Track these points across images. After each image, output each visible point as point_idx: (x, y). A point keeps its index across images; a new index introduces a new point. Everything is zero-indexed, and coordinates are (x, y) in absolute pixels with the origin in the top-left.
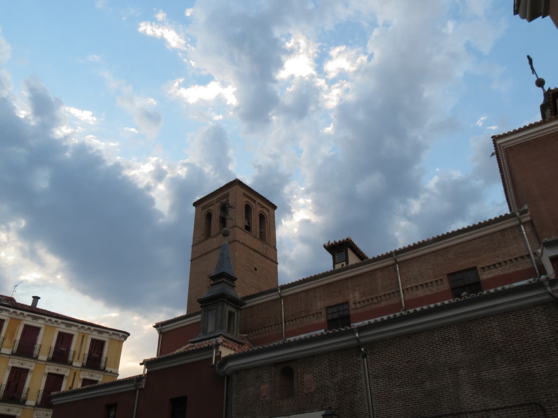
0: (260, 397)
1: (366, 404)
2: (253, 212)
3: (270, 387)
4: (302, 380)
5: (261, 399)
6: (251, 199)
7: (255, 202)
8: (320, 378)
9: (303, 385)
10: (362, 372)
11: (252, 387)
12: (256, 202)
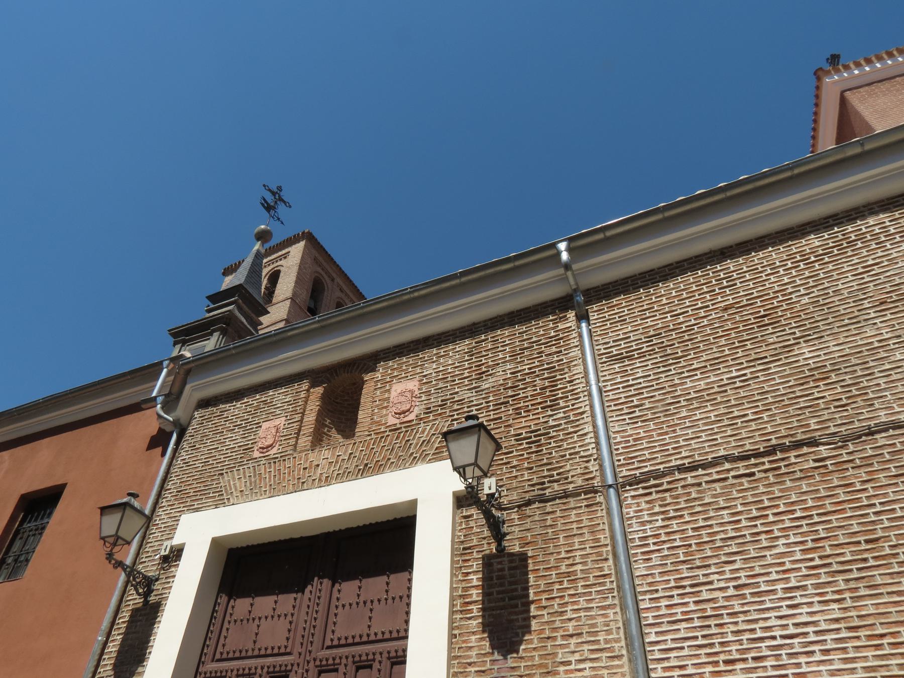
1: (589, 428)
2: (326, 293)
3: (288, 424)
4: (386, 396)
6: (327, 273)
7: (333, 280)
8: (441, 385)
9: (386, 407)
10: (576, 352)
12: (336, 281)
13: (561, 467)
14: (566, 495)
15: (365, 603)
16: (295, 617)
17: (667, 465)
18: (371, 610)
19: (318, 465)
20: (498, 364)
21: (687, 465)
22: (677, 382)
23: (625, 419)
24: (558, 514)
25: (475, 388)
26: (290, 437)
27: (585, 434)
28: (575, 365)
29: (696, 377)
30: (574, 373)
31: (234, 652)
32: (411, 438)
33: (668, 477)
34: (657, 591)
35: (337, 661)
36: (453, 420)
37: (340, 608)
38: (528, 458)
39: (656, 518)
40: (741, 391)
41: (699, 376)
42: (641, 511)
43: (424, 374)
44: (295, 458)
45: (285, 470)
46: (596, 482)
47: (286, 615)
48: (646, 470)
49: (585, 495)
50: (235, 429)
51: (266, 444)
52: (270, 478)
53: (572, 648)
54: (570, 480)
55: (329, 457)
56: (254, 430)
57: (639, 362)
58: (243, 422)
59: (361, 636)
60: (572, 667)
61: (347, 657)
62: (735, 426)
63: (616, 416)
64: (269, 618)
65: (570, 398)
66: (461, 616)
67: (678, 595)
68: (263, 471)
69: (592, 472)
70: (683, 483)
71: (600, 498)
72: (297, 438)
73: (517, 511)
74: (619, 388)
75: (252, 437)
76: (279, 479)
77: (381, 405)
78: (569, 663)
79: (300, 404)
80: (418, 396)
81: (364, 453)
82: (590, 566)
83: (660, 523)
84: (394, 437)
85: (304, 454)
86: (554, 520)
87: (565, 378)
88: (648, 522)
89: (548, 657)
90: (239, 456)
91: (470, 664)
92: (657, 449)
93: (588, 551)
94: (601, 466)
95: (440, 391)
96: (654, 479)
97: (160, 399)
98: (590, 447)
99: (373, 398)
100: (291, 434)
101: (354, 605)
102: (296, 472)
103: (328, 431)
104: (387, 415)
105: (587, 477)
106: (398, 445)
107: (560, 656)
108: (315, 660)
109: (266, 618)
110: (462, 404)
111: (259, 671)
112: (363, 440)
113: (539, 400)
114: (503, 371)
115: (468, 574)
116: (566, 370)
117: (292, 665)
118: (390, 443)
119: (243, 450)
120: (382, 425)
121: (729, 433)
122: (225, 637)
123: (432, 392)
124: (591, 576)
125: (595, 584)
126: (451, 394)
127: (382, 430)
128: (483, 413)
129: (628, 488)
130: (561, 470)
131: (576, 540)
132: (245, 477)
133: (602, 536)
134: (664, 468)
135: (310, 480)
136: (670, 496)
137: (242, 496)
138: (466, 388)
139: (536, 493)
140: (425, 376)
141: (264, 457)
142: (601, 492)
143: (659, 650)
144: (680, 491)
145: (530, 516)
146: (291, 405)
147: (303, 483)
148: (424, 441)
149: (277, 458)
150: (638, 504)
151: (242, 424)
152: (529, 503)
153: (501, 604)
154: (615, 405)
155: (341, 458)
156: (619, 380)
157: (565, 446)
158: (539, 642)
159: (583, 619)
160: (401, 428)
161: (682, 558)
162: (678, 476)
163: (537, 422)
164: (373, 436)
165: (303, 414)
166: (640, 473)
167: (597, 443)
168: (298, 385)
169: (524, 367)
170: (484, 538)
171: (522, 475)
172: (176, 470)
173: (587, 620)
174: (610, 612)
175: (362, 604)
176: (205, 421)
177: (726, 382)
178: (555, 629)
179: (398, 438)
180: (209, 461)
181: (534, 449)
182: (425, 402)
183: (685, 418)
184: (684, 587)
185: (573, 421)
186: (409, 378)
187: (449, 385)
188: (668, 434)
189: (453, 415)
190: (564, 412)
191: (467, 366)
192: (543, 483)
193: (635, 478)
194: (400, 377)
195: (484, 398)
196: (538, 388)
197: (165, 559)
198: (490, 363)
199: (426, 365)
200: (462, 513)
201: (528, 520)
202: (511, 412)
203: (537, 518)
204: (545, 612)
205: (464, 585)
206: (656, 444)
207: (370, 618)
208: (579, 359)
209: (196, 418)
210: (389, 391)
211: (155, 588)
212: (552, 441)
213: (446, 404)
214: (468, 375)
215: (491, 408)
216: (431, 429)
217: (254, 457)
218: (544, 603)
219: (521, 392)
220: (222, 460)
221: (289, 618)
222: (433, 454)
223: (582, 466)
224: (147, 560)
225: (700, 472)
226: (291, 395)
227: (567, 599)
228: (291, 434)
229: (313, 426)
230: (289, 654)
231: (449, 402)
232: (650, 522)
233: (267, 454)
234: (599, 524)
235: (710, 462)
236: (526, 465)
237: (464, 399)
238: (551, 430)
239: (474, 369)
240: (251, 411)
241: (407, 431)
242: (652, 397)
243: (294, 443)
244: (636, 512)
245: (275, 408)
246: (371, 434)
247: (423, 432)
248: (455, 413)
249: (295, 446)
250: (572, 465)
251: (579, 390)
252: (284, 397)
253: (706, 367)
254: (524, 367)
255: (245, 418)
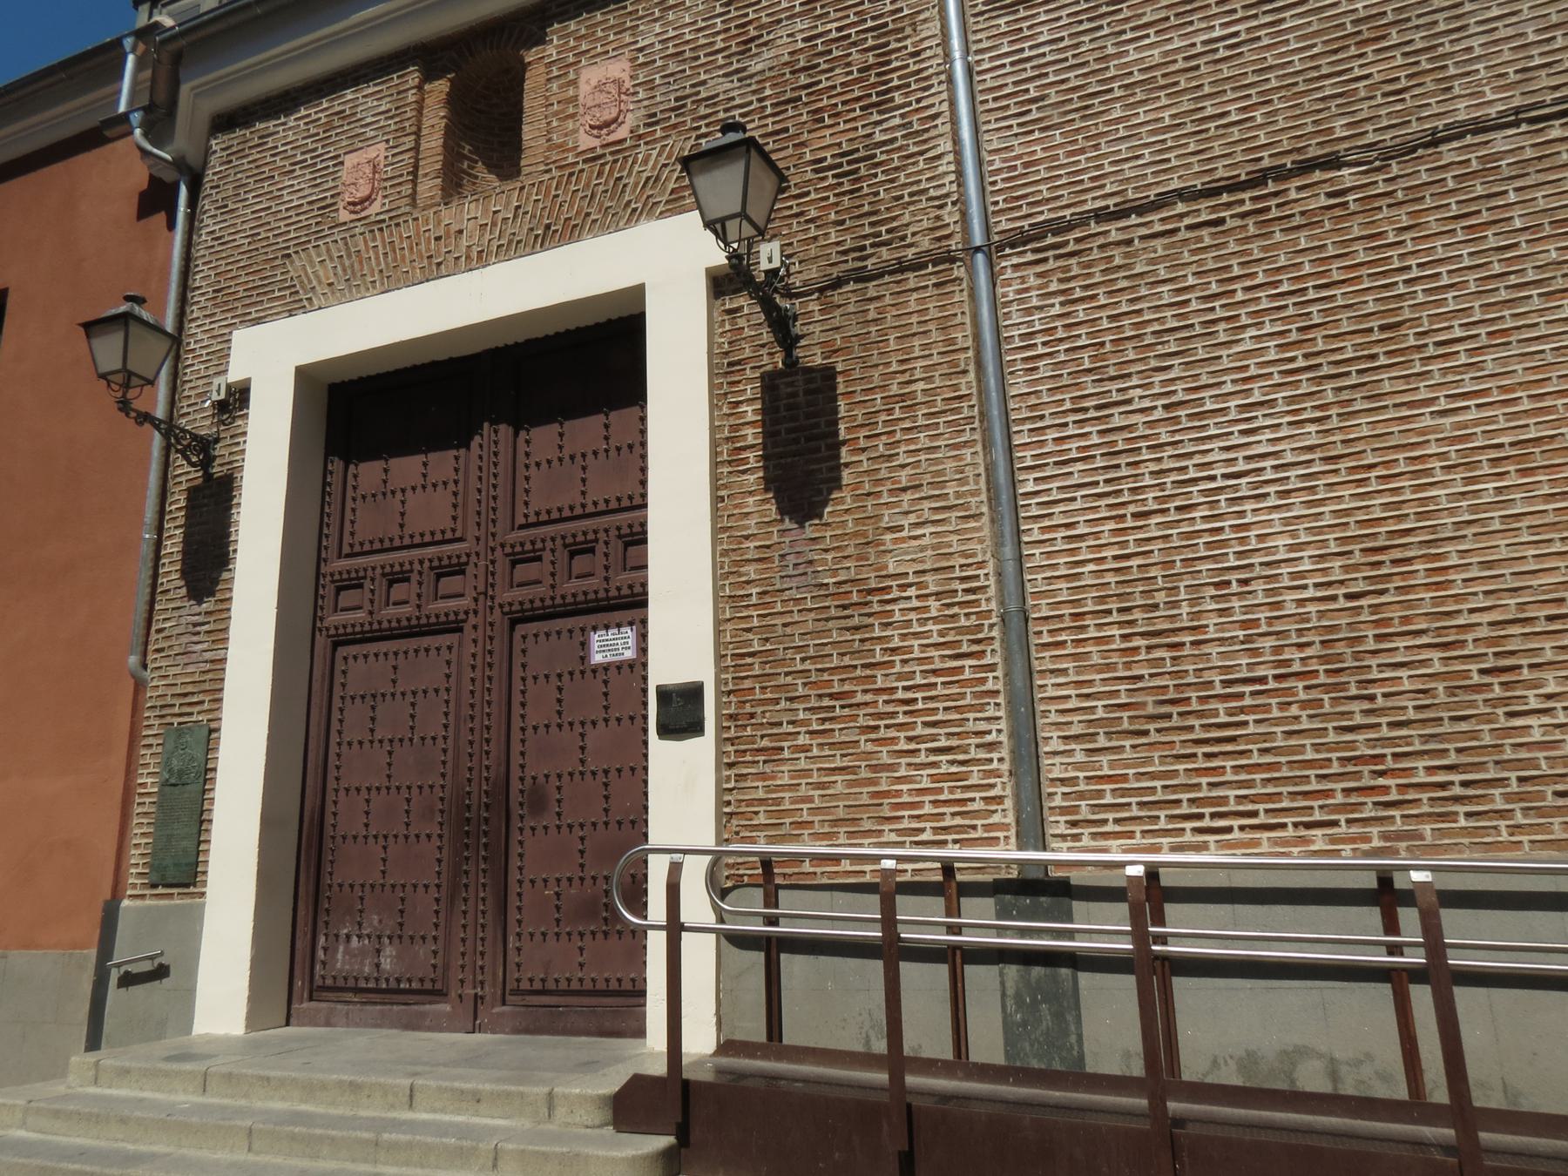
0: (337, 210)
1: (945, 145)
4: (571, 93)
5: (344, 216)
8: (673, 68)
9: (573, 116)
11: (298, 173)
13: (894, 219)
14: (902, 267)
15: (572, 457)
16: (461, 485)
17: (1078, 210)
18: (584, 468)
19: (461, 232)
20: (779, 21)
21: (1112, 209)
22: (1111, 50)
23: (1011, 126)
24: (888, 300)
25: (737, 71)
26: (401, 180)
27: (939, 157)
28: (925, 21)
29: (1147, 41)
30: (923, 35)
31: (371, 542)
32: (625, 174)
33: (1077, 230)
34: (1042, 417)
35: (539, 545)
36: (698, 137)
37: (533, 468)
38: (837, 204)
39: (1052, 301)
40: (1224, 66)
41: (1153, 39)
42: (1027, 290)
43: (639, 46)
44: (416, 219)
45: (402, 242)
46: (954, 244)
47: (445, 483)
48: (1041, 218)
49: (934, 266)
50: (294, 170)
51: (359, 195)
52: (377, 258)
53: (905, 507)
54: (909, 241)
55: (479, 215)
56: (331, 170)
57: (1046, 12)
58: (308, 156)
59: (572, 508)
60: (905, 534)
61: (553, 539)
62: (1204, 136)
63: (996, 120)
64: (419, 489)
65: (913, 87)
66: (730, 469)
67: (1075, 422)
68: (362, 247)
69: (948, 225)
70: (1101, 241)
71: (959, 271)
72: (414, 182)
73: (818, 299)
74: (1004, 66)
75: (331, 184)
76: (395, 260)
77: (563, 111)
78: (900, 528)
79: (409, 115)
80: (632, 90)
81: (541, 206)
82: (938, 383)
83: (1057, 310)
84: (592, 172)
85: (432, 211)
86: (880, 311)
87: (906, 47)
88: (1037, 308)
89: (867, 521)
90: (313, 221)
91: (747, 537)
92: (1064, 181)
93: (936, 359)
94: (964, 215)
95: (672, 80)
96: (1053, 235)
97: (136, 118)
98: (947, 180)
99: (547, 98)
100: (402, 175)
101: (555, 463)
102: (423, 247)
103: (469, 167)
104: (575, 131)
105: (939, 234)
106: (601, 188)
107: (886, 518)
108: (503, 546)
109: (414, 489)
110: (715, 104)
111: (417, 566)
112: (537, 181)
113: (857, 94)
114: (788, 36)
115: (738, 404)
116: (908, 31)
117: (468, 555)
118: (587, 185)
119: (319, 209)
120: (568, 150)
121: (1192, 148)
122: (353, 522)
123: (657, 82)
124: (939, 398)
125: (944, 412)
126: (693, 86)
127: (570, 160)
128: (753, 121)
129: (1008, 251)
130: (895, 224)
131: (917, 342)
132: (331, 259)
133: (960, 335)
134: (1072, 215)
135: (450, 258)
136: (1079, 263)
137: (333, 293)
138: (721, 73)
139: (850, 265)
140: (641, 50)
141: (359, 220)
142: (961, 260)
143: (1038, 504)
144: (1096, 254)
145: (839, 306)
146: (391, 118)
147: (439, 264)
148: (648, 178)
149: (384, 221)
150: (1023, 279)
151: (306, 160)
152: (838, 283)
153: (794, 447)
154: (995, 99)
155: (500, 216)
156: (1006, 49)
157: (903, 180)
158: (854, 502)
159: (924, 465)
160: (604, 155)
161: (1087, 365)
162: (1094, 228)
163: (851, 135)
164: (555, 173)
165: (418, 134)
166: (1030, 225)
167: (960, 173)
168: (398, 77)
169: (829, 26)
170: (763, 346)
171: (826, 234)
172: (202, 253)
173: (930, 465)
174: (967, 452)
175: (567, 460)
176: (233, 158)
177: (1199, 49)
178: (879, 481)
179: (600, 174)
180: (259, 234)
181: (847, 187)
182: (646, 103)
183: (1118, 120)
184: (1086, 410)
185: (917, 132)
186: (611, 54)
187: (687, 67)
188: (1085, 153)
189: (699, 128)
190: (903, 116)
191: (719, 27)
192: (863, 248)
193: (1022, 233)
194: (593, 53)
195: (754, 92)
196: (855, 68)
197: (222, 407)
198: (765, 20)
199: (642, 28)
200: (724, 304)
201: (837, 313)
202: (804, 118)
203: (851, 308)
204: (863, 457)
205: (732, 421)
206: (1062, 172)
207: (584, 480)
208: (934, 7)
209: (215, 152)
210: (574, 83)
211: (216, 453)
212: (879, 170)
213: (684, 106)
214: (722, 45)
215: (769, 111)
216: (659, 155)
217: (342, 220)
218: (862, 443)
219: (823, 77)
220: (284, 229)
221: (451, 487)
222: (667, 202)
223: (932, 215)
224: (191, 410)
225: (1134, 219)
226: (388, 99)
227: (898, 436)
228: (402, 175)
229: (441, 158)
230: (460, 540)
231: (689, 101)
232: (1041, 308)
233: (363, 214)
234: (956, 315)
235: (1153, 202)
236: (833, 217)
237: (717, 95)
238: (878, 151)
239: (734, 32)
240: (318, 134)
241: (615, 161)
242: (1063, 81)
243: (410, 191)
244: (1019, 292)
245: (362, 126)
246: (551, 170)
247: (645, 162)
248: (702, 123)
249: (413, 196)
250: (913, 214)
251: (931, 71)
252: (375, 103)
253: (1167, 19)
254: (829, 26)
255: (310, 147)
